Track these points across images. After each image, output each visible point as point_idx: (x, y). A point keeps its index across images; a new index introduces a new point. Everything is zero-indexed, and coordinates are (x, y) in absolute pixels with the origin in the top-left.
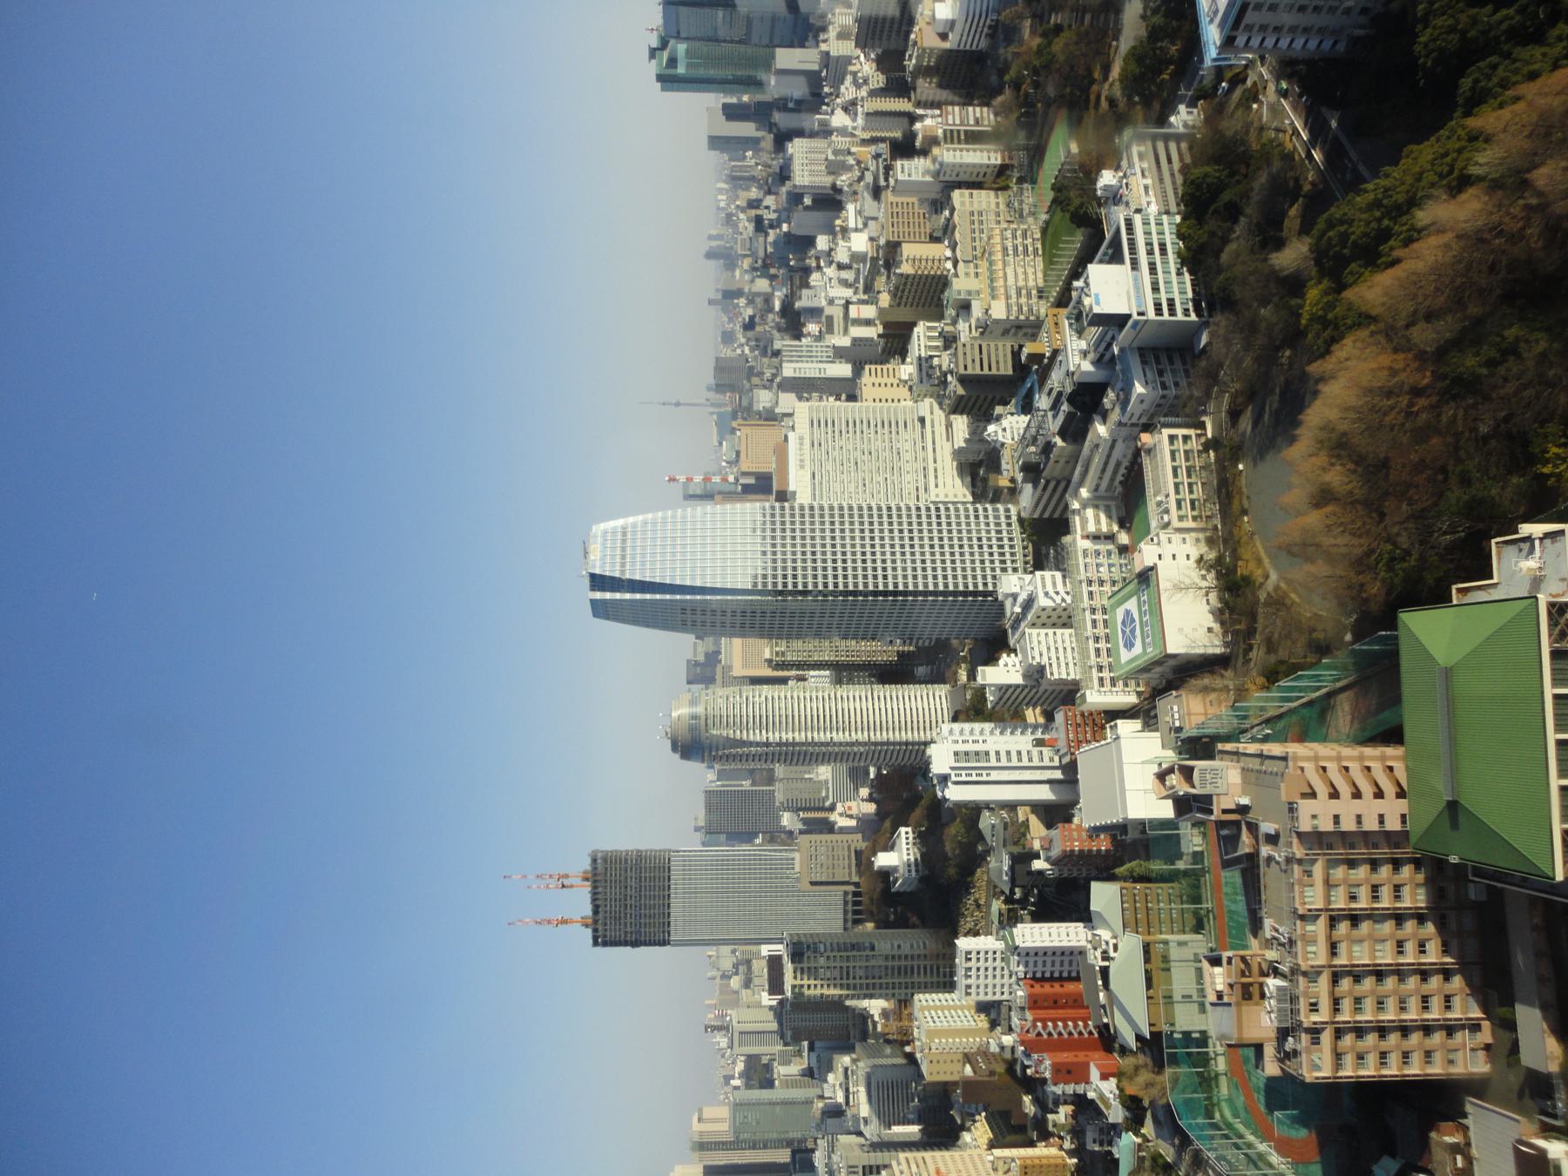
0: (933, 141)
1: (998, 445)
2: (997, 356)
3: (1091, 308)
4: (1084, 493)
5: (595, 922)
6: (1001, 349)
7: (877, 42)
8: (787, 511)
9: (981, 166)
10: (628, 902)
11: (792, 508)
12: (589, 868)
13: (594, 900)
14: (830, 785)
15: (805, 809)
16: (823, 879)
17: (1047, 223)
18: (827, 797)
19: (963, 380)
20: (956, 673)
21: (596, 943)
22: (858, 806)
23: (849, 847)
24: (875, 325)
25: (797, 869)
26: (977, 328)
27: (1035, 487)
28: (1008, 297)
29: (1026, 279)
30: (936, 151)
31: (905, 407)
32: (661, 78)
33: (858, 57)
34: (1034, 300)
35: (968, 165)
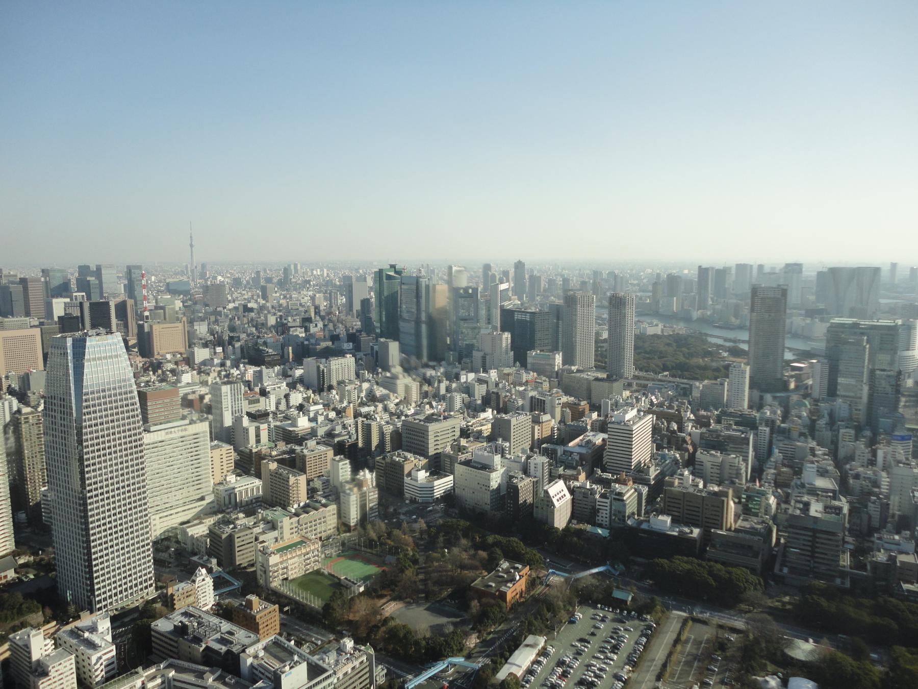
0: (360, 485)
1: (193, 578)
2: (247, 553)
3: (283, 673)
4: (172, 674)
6: (252, 553)
7: (405, 431)
8: (138, 431)
9: (349, 515)
11: (140, 434)
17: (323, 574)
19: (231, 538)
20: (25, 554)
24: (257, 447)
26: (263, 547)
27: (170, 633)
28: (281, 563)
29: (292, 569)
30: (356, 489)
31: (209, 481)
32: (381, 271)
33: (397, 398)
34: (281, 577)
35: (349, 509)
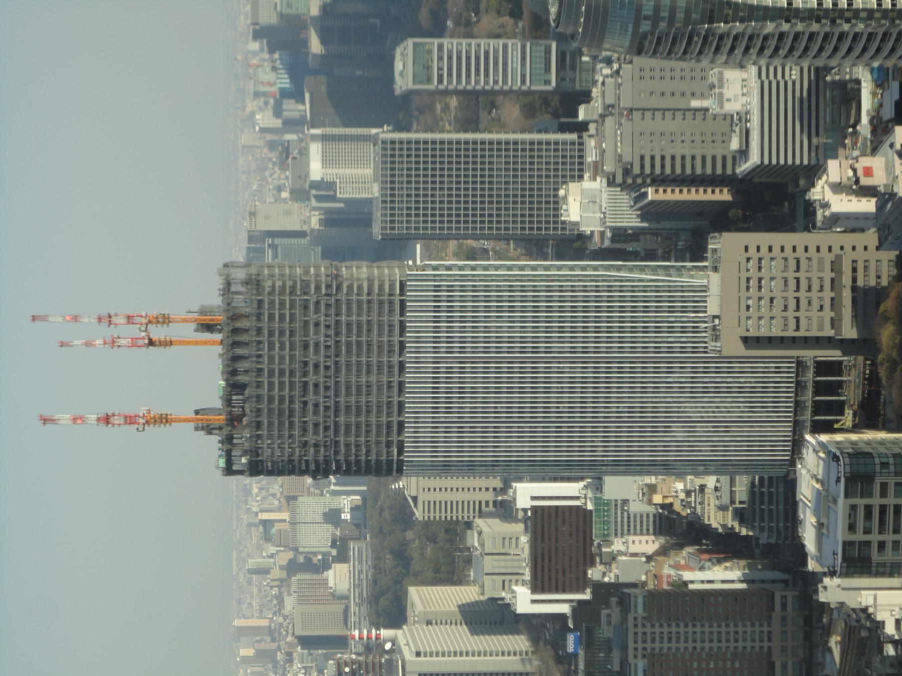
5: (234, 420)
10: (311, 378)
12: (216, 300)
13: (231, 373)
14: (754, 124)
15: (660, 181)
16: (776, 331)
18: (744, 153)
21: (229, 470)
22: (889, 168)
23: (836, 266)
25: (713, 308)
